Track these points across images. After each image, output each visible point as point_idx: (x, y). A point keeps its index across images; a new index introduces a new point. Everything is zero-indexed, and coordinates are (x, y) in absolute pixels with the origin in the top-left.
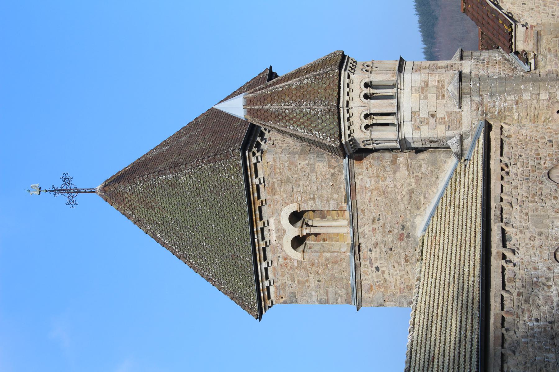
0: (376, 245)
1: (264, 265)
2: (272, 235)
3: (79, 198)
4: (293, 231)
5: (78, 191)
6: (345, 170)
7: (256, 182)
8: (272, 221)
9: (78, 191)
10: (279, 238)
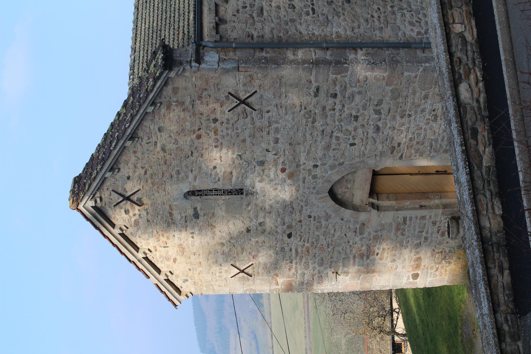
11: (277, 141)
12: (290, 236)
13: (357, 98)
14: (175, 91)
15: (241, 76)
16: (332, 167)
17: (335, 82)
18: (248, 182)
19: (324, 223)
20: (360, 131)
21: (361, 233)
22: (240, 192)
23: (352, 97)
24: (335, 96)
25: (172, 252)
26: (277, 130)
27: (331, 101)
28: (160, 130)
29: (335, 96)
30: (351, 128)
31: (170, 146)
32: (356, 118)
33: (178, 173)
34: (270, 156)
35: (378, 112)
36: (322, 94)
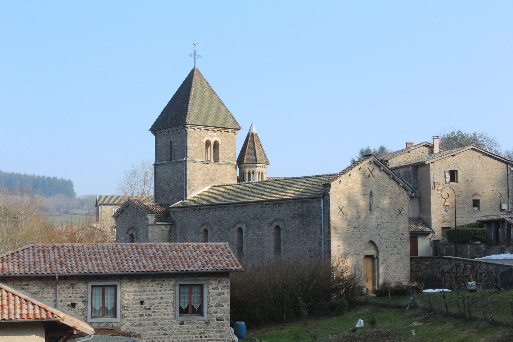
0: (208, 170)
1: (203, 129)
2: (211, 133)
3: (192, 59)
4: (212, 142)
5: (195, 59)
6: (232, 162)
7: (230, 131)
8: (215, 134)
9: (195, 59)
10: (210, 136)
11: (388, 222)
12: (355, 228)
13: (400, 247)
14: (403, 192)
15: (407, 212)
16: (379, 241)
17: (405, 239)
18: (375, 213)
19: (359, 240)
20: (391, 249)
21: (354, 254)
22: (370, 210)
23: (400, 245)
24: (401, 240)
25: (350, 185)
26: (391, 222)
27: (399, 239)
28: (392, 186)
29: (401, 240)
30: (392, 246)
31: (388, 189)
32: (395, 247)
33: (379, 190)
34: (383, 220)
35: (397, 254)
36: (402, 236)
